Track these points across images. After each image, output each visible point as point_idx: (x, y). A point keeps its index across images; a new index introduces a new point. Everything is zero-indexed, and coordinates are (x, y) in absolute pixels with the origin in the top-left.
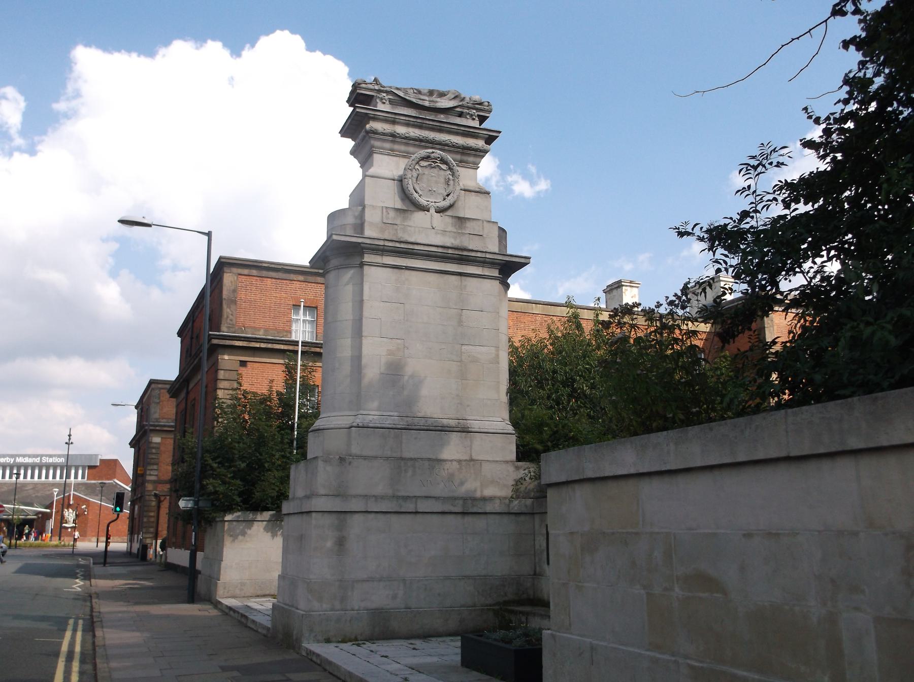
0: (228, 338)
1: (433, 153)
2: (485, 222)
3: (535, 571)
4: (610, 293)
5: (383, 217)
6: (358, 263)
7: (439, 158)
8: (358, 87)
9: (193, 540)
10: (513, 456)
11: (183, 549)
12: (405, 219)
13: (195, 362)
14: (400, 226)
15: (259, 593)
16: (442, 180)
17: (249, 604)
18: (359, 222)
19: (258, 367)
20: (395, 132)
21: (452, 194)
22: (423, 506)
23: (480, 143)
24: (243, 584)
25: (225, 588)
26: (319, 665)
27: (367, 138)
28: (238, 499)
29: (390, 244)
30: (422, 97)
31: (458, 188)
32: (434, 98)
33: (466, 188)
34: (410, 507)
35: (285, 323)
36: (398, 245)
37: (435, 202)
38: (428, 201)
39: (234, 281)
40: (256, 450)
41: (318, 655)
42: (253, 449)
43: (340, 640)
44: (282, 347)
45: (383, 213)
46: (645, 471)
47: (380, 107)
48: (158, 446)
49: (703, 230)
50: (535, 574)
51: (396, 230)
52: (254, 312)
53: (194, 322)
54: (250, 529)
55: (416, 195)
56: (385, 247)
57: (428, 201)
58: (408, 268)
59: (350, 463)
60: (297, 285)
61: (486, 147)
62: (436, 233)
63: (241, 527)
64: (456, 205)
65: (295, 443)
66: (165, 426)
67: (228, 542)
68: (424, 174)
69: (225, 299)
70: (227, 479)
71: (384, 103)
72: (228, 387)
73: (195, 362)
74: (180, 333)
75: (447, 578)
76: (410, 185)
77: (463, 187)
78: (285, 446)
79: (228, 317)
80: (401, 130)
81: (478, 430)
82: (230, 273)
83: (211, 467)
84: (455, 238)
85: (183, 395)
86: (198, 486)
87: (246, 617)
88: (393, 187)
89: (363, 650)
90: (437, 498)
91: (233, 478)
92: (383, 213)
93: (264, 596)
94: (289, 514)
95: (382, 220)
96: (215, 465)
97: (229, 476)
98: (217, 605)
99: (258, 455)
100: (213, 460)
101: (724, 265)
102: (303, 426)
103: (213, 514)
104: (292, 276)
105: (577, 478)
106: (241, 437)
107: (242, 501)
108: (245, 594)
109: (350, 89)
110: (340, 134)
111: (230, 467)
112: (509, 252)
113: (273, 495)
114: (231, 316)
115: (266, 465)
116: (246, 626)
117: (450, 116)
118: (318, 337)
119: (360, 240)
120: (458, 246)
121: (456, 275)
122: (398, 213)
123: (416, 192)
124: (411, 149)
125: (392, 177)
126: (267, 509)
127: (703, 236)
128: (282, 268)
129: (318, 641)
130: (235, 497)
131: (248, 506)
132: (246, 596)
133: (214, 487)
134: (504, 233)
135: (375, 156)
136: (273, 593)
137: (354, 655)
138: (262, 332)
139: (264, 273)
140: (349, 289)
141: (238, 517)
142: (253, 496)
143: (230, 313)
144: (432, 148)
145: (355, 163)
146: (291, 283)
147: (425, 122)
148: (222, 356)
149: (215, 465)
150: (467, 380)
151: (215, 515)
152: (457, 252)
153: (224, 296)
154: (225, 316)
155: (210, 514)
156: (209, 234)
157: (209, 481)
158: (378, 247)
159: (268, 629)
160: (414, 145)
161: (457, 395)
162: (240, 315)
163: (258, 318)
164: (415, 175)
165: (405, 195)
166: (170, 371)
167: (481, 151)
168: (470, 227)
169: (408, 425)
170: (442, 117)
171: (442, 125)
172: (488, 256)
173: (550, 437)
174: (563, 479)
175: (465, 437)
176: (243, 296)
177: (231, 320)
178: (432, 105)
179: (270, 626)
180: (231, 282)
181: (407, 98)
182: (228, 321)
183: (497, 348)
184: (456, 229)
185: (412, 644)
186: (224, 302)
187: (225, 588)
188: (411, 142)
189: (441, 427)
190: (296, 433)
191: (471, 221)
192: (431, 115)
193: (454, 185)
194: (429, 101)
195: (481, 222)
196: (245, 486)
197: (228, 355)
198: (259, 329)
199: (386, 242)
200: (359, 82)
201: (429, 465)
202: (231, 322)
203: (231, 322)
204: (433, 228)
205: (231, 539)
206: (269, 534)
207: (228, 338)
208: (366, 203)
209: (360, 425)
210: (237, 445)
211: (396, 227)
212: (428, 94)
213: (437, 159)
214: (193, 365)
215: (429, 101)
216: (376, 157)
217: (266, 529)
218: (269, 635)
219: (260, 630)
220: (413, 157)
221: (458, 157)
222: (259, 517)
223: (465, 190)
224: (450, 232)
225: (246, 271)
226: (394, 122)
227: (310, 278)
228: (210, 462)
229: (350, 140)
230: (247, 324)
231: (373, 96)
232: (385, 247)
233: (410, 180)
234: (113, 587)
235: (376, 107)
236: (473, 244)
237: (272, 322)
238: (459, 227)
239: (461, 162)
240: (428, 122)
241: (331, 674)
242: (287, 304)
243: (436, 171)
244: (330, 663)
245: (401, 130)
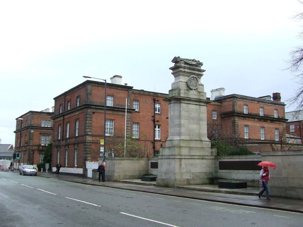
10: (210, 147)
22: (195, 157)
29: (186, 98)
41: (191, 188)
48: (33, 133)
58: (190, 104)
66: (35, 127)
75: (200, 173)
76: (189, 83)
80: (186, 70)
165: (188, 86)
168: (201, 94)
225: (94, 85)
230: (95, 101)
236: (202, 98)
243: (194, 80)
245: (186, 70)
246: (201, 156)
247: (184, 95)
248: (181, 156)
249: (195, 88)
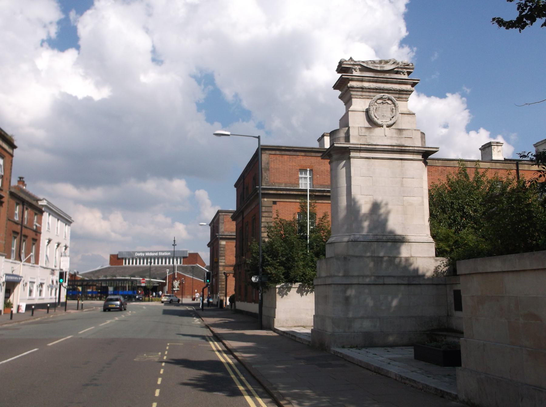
0: (266, 189)
1: (384, 96)
2: (413, 131)
3: (448, 314)
4: (484, 150)
5: (359, 133)
6: (348, 157)
7: (387, 98)
8: (342, 64)
9: (260, 297)
10: (434, 254)
11: (246, 303)
12: (370, 132)
13: (248, 202)
14: (368, 136)
15: (296, 325)
16: (389, 110)
17: (293, 330)
18: (347, 136)
19: (282, 204)
20: (363, 86)
21: (395, 117)
22: (387, 281)
23: (409, 87)
24: (287, 320)
25: (278, 322)
26: (341, 358)
27: (348, 91)
28: (282, 277)
30: (376, 65)
31: (398, 113)
32: (382, 65)
33: (402, 112)
34: (381, 281)
36: (368, 147)
37: (386, 122)
38: (382, 122)
40: (290, 251)
42: (289, 250)
43: (349, 347)
44: (295, 193)
45: (359, 130)
46: (506, 270)
47: (355, 73)
48: (224, 247)
49: (533, 155)
50: (448, 316)
51: (366, 139)
53: (244, 180)
54: (290, 292)
55: (375, 119)
56: (361, 148)
57: (382, 122)
58: (373, 158)
59: (349, 260)
60: (301, 158)
62: (388, 138)
63: (285, 291)
64: (397, 122)
65: (308, 246)
67: (278, 297)
68: (379, 107)
69: (263, 168)
70: (276, 267)
71: (356, 71)
73: (248, 202)
74: (236, 186)
76: (372, 114)
77: (400, 112)
78: (304, 248)
79: (265, 178)
80: (366, 85)
82: (265, 154)
83: (267, 259)
84: (397, 140)
85: (240, 219)
86: (261, 270)
87: (295, 336)
88: (363, 115)
89: (363, 351)
90: (394, 277)
91: (279, 266)
92: (359, 130)
93: (298, 326)
94: (317, 285)
95: (359, 134)
96: (269, 259)
97: (277, 265)
98: (275, 330)
99: (291, 253)
100: (268, 256)
101: (543, 173)
102: (312, 237)
103: (270, 284)
104: (298, 153)
105: (474, 272)
106: (281, 243)
107: (284, 278)
108: (288, 325)
109: (338, 64)
110: (333, 88)
111: (277, 260)
112: (427, 146)
113: (300, 274)
114: (267, 178)
115: (296, 258)
116: (295, 341)
117: (392, 74)
118: (314, 186)
119: (348, 146)
120: (399, 144)
121: (399, 160)
122: (367, 130)
123: (376, 117)
124: (372, 94)
125: (363, 111)
126: (297, 282)
127: (533, 158)
128: (293, 149)
129: (339, 347)
130: (281, 276)
131: (287, 280)
132: (289, 326)
133: (270, 271)
134: (424, 135)
135: (353, 99)
136: (302, 325)
137: (359, 353)
138: (283, 185)
139: (283, 153)
140: (344, 169)
141: (283, 286)
142: (290, 275)
143: (266, 175)
144: (383, 93)
145: (341, 103)
147: (378, 79)
148: (263, 199)
149: (269, 259)
150: (407, 215)
151: (271, 285)
152: (399, 148)
153: (263, 167)
155: (269, 284)
156: (259, 138)
157: (268, 267)
158: (357, 148)
159: (309, 342)
160: (373, 92)
161: (402, 223)
163: (281, 177)
164: (375, 108)
165: (369, 119)
166: (233, 207)
167: (409, 91)
168: (405, 134)
169: (377, 240)
170: (387, 75)
171: (388, 80)
172: (416, 148)
173: (454, 243)
174: (467, 272)
175: (408, 245)
176: (272, 166)
177: (267, 179)
178: (382, 69)
179: (310, 340)
180: (266, 159)
181: (368, 67)
182: (266, 180)
183: (423, 197)
185: (386, 349)
187: (278, 322)
188: (372, 90)
190: (308, 241)
192: (381, 75)
193: (396, 112)
195: (410, 131)
196: (285, 270)
197: (267, 198)
198: (282, 183)
199: (361, 145)
200: (343, 61)
203: (267, 181)
204: (386, 136)
205: (281, 297)
206: (299, 294)
207: (266, 189)
208: (349, 126)
209: (353, 240)
210: (279, 248)
211: (366, 137)
212: (379, 63)
213: (386, 99)
214: (246, 204)
216: (354, 100)
217: (298, 292)
218: (310, 345)
219: (304, 343)
220: (374, 98)
221: (397, 96)
222: (294, 286)
223: (402, 114)
224: (394, 137)
225: (273, 152)
227: (308, 154)
228: (267, 257)
229: (338, 91)
231: (350, 68)
232: (361, 148)
233: (372, 111)
234: (215, 322)
235: (352, 74)
236: (407, 143)
239: (398, 98)
240: (380, 79)
241: (350, 362)
242: (296, 169)
243: (386, 105)
244: (348, 357)
245: (366, 85)
246: (404, 277)
247: (359, 140)
249: (391, 122)
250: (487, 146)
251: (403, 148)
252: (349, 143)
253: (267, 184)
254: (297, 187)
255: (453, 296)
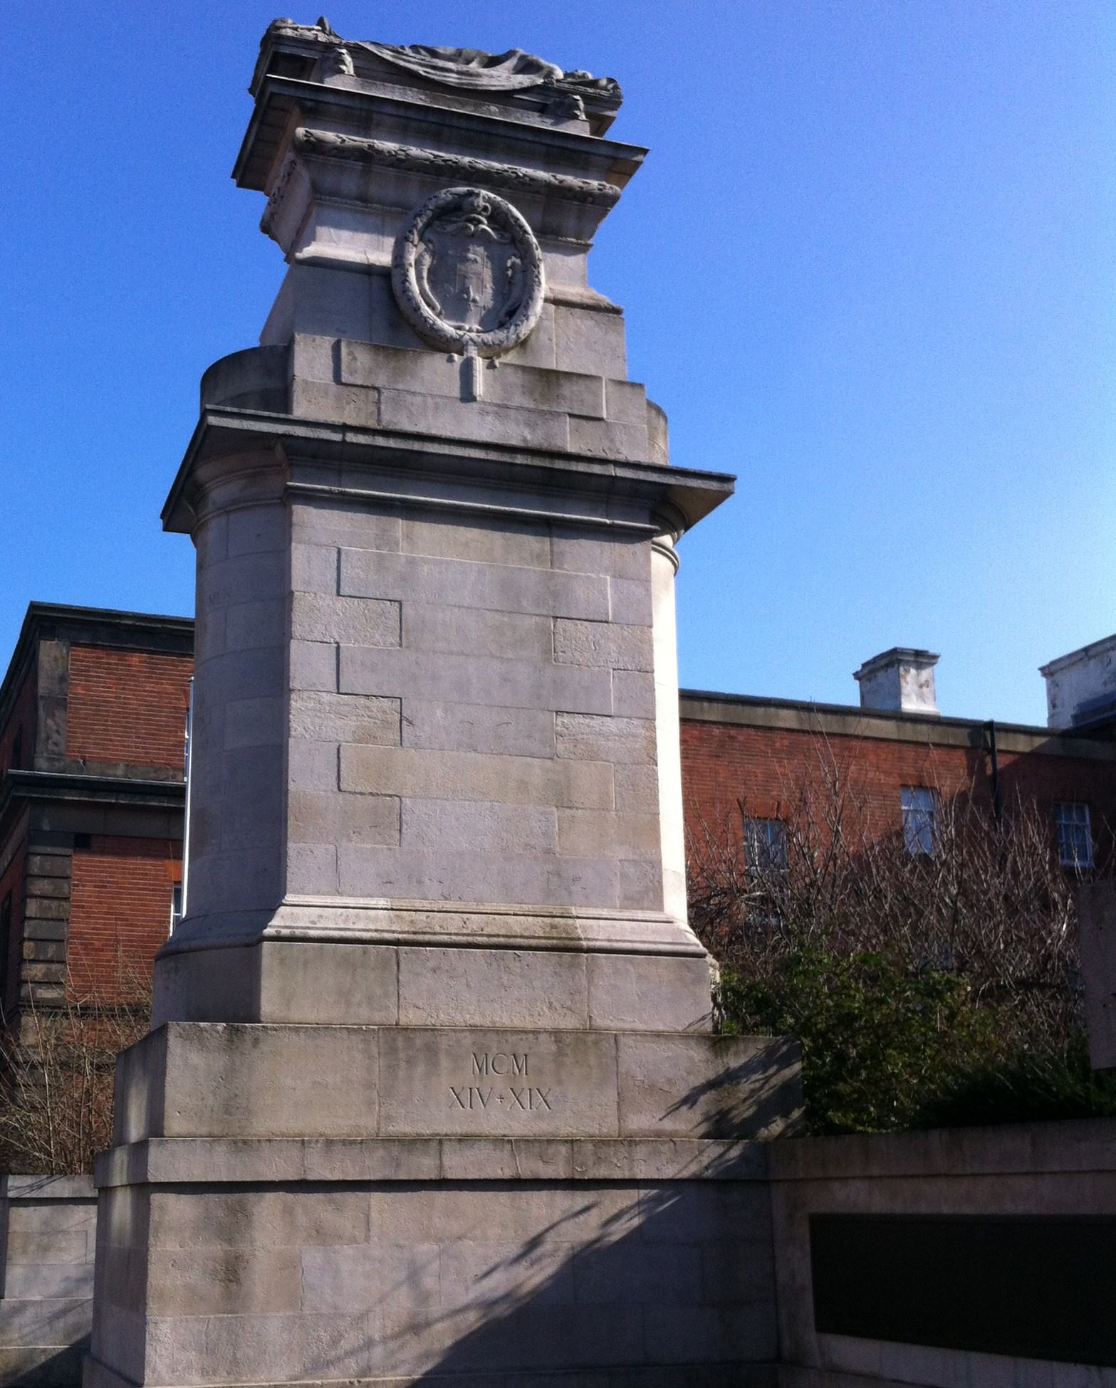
4: (869, 680)
35: (170, 750)
36: (380, 441)
39: (63, 657)
52: (103, 725)
61: (611, 188)
62: (483, 413)
64: (533, 338)
72: (49, 893)
81: (606, 944)
84: (532, 426)
114: (55, 737)
122: (381, 358)
138: (122, 767)
143: (55, 728)
146: (182, 662)
154: (43, 735)
162: (76, 733)
177: (56, 744)
182: (50, 746)
184: (535, 400)
186: (41, 704)
189: (504, 936)
191: (575, 379)
194: (458, 72)
201: (474, 1043)
202: (56, 749)
203: (56, 749)
215: (458, 72)
224: (517, 408)
226: (365, 127)
237: (143, 748)
238: (542, 395)
248: (242, 1144)
250: (883, 662)
251: (560, 465)
252: (282, 416)
253: (56, 764)
254: (174, 777)
255: (808, 1248)
